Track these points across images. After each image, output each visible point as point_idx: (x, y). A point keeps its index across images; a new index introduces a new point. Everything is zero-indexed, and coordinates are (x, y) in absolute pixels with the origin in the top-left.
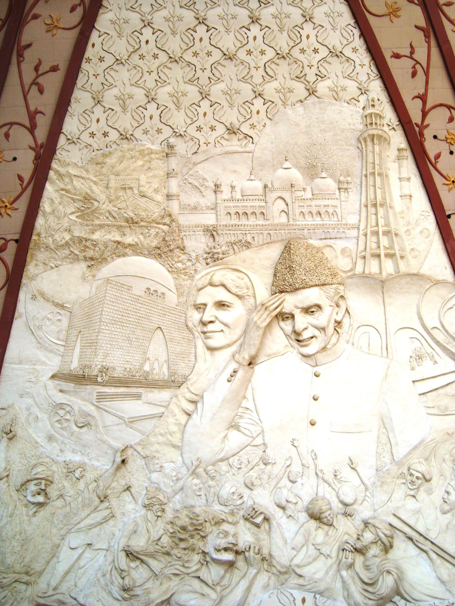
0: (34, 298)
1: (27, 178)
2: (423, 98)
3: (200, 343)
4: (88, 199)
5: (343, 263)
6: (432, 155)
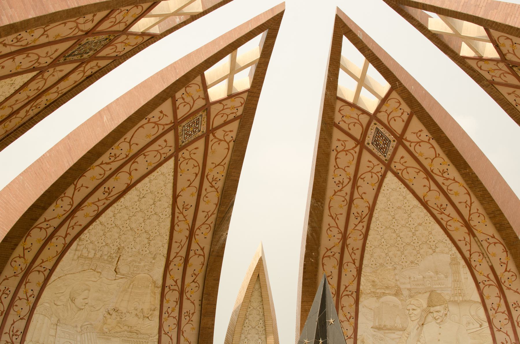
0: (363, 307)
1: (355, 276)
2: (470, 251)
3: (409, 319)
4: (373, 281)
5: (447, 298)
6: (474, 265)
